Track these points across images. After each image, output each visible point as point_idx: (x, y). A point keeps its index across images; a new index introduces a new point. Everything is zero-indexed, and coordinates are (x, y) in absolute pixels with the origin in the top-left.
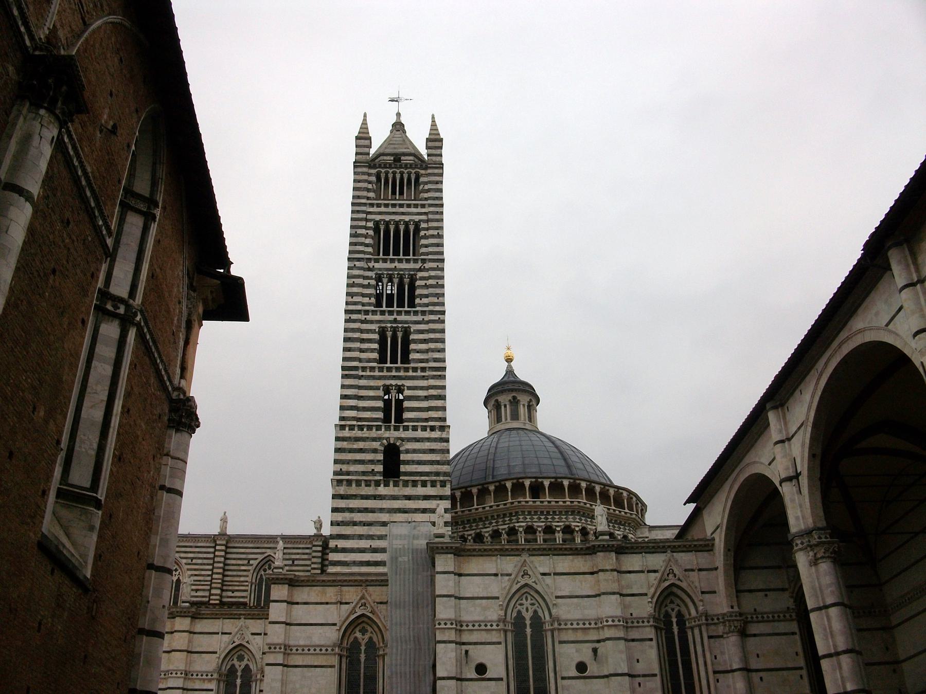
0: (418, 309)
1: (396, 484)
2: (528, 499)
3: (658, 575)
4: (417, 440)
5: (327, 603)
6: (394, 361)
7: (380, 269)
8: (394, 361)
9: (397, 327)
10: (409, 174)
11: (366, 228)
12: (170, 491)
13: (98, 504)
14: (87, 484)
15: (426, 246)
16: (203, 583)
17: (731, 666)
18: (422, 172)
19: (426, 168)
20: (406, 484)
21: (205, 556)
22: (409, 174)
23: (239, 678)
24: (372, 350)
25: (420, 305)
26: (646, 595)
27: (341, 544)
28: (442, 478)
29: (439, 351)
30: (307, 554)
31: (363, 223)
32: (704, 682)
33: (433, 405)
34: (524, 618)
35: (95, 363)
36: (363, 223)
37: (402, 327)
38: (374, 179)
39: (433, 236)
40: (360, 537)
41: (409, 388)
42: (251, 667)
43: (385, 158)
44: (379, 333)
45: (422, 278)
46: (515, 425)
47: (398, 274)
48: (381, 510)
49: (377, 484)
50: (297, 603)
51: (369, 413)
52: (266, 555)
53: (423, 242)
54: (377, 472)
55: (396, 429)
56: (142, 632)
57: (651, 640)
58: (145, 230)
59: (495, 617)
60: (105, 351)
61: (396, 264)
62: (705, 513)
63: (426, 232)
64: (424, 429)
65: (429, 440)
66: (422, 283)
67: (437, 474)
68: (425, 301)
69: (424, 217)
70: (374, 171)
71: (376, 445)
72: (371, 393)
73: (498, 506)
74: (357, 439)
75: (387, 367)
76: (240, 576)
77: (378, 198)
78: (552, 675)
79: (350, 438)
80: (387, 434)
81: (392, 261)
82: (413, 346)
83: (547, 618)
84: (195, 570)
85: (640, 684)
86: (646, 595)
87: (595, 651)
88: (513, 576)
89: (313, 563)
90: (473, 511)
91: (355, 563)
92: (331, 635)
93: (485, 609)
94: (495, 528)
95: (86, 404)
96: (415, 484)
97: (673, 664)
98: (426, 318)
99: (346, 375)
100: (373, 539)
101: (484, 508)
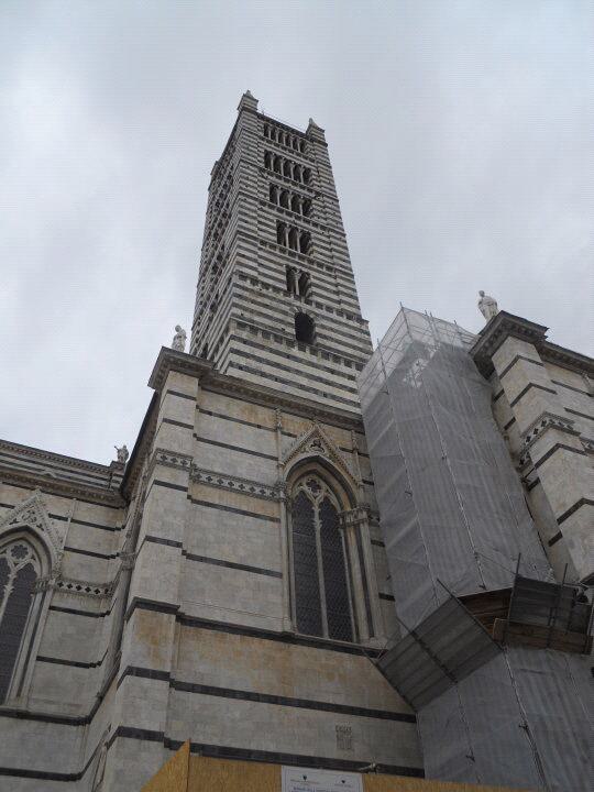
1: (313, 352)
23: (10, 582)
41: (314, 277)
42: (37, 569)
48: (298, 372)
50: (210, 413)
72: (273, 266)
80: (298, 303)
96: (337, 359)
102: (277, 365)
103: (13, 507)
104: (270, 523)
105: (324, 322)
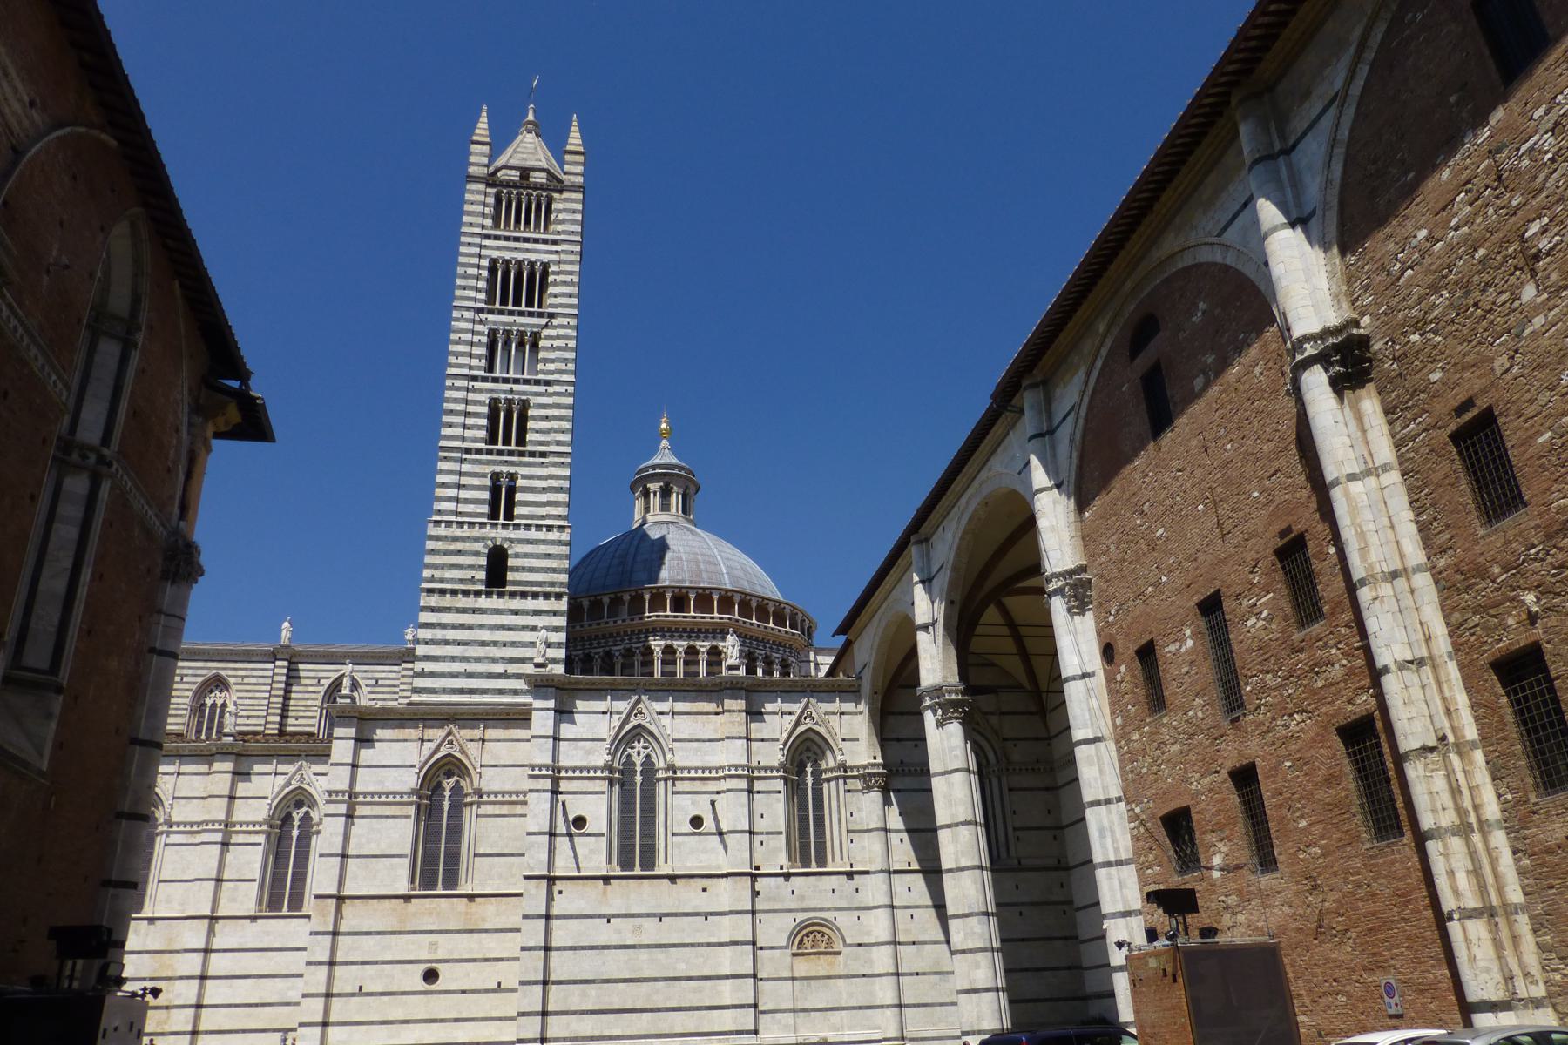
0: (541, 377)
1: (501, 595)
2: (668, 613)
3: (794, 718)
4: (530, 542)
5: (405, 741)
6: (507, 442)
7: (495, 323)
8: (507, 442)
9: (513, 400)
10: (539, 196)
11: (479, 267)
12: (163, 653)
13: (59, 690)
14: (45, 665)
15: (555, 296)
16: (257, 708)
17: (868, 825)
18: (556, 195)
19: (560, 192)
20: (513, 594)
21: (261, 673)
22: (539, 196)
23: (296, 828)
24: (479, 427)
25: (543, 372)
26: (777, 740)
27: (429, 667)
28: (557, 590)
29: (563, 432)
30: (395, 672)
31: (475, 260)
32: (836, 843)
33: (552, 499)
34: (634, 764)
35: (56, 525)
36: (475, 260)
37: (520, 400)
38: (491, 200)
39: (565, 283)
40: (453, 659)
41: (524, 477)
43: (509, 172)
44: (489, 406)
45: (548, 338)
46: (665, 517)
47: (518, 331)
48: (481, 627)
49: (477, 594)
51: (472, 506)
52: (342, 672)
54: (479, 580)
55: (505, 526)
56: (120, 815)
57: (780, 792)
58: (124, 360)
59: (600, 763)
60: (71, 511)
62: (856, 646)
63: (556, 277)
64: (539, 527)
65: (544, 542)
66: (547, 343)
67: (552, 584)
68: (551, 367)
69: (554, 257)
70: (492, 191)
71: (478, 546)
72: (476, 481)
73: (632, 620)
74: (455, 539)
75: (498, 450)
76: (308, 699)
78: (662, 830)
79: (446, 537)
81: (511, 313)
82: (530, 424)
83: (662, 765)
84: (247, 691)
85: (762, 843)
86: (777, 740)
87: (713, 803)
88: (624, 715)
89: (402, 683)
90: (602, 625)
91: (444, 691)
92: (409, 780)
93: (589, 752)
94: (628, 646)
95: (46, 572)
96: (524, 595)
97: (803, 820)
98: (551, 389)
99: (445, 458)
100: (469, 662)
101: (615, 622)
102: (462, 626)
103: (287, 774)
104: (404, 820)
105: (519, 549)
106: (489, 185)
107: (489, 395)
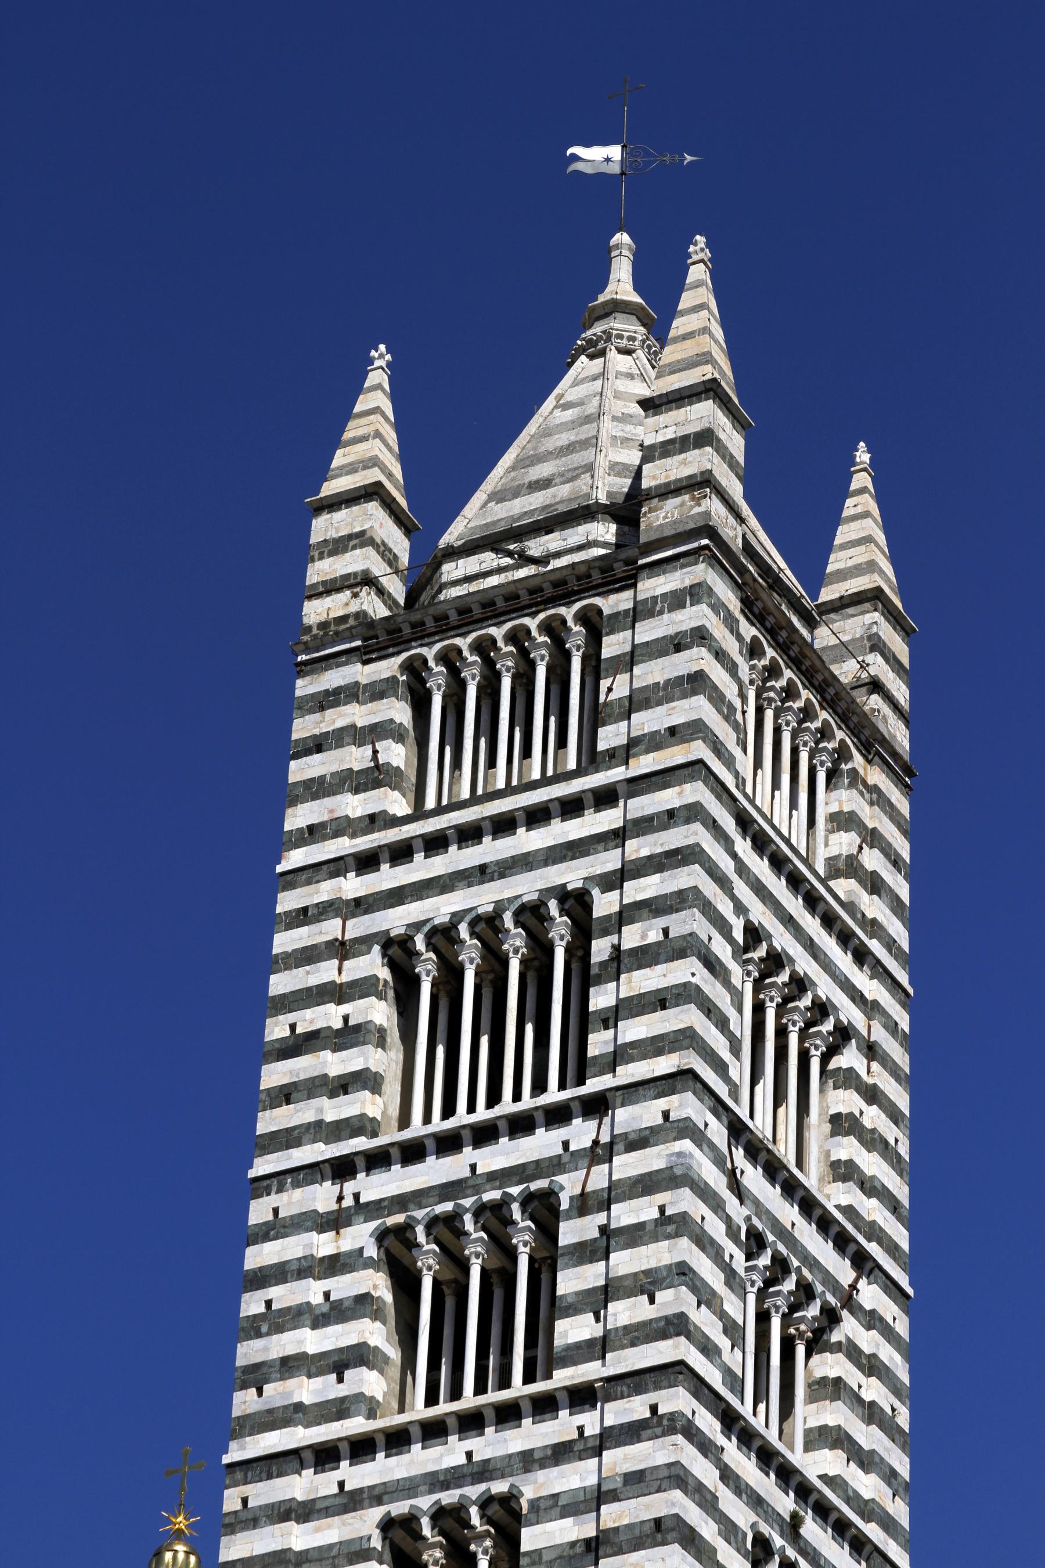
0: (564, 1377)
7: (401, 1202)
10: (555, 630)
31: (326, 972)
36: (326, 972)
37: (486, 1503)
45: (584, 1205)
53: (601, 998)
61: (468, 1154)
69: (609, 861)
70: (388, 668)
77: (419, 813)
106: (366, 655)
107: (375, 1514)
